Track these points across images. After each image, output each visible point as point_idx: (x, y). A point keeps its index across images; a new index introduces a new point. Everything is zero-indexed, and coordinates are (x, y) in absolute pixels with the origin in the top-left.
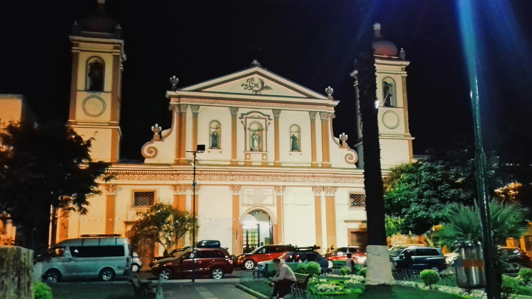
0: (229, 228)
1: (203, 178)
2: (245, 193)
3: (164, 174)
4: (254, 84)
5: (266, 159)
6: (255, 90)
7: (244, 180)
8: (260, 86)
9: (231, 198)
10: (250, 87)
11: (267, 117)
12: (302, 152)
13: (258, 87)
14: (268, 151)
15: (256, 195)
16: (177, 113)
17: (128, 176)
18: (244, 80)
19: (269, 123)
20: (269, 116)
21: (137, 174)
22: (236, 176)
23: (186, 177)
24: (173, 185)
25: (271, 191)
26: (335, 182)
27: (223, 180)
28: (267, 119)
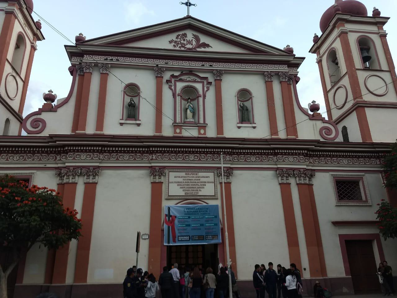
0: (143, 235)
2: (172, 179)
3: (47, 152)
4: (187, 41)
5: (205, 134)
6: (188, 47)
7: (170, 159)
8: (194, 43)
9: (150, 186)
12: (255, 124)
13: (192, 45)
14: (206, 123)
16: (79, 75)
18: (173, 36)
20: (206, 78)
21: (5, 153)
23: (78, 156)
24: (56, 168)
25: (211, 175)
26: (310, 163)
28: (205, 83)
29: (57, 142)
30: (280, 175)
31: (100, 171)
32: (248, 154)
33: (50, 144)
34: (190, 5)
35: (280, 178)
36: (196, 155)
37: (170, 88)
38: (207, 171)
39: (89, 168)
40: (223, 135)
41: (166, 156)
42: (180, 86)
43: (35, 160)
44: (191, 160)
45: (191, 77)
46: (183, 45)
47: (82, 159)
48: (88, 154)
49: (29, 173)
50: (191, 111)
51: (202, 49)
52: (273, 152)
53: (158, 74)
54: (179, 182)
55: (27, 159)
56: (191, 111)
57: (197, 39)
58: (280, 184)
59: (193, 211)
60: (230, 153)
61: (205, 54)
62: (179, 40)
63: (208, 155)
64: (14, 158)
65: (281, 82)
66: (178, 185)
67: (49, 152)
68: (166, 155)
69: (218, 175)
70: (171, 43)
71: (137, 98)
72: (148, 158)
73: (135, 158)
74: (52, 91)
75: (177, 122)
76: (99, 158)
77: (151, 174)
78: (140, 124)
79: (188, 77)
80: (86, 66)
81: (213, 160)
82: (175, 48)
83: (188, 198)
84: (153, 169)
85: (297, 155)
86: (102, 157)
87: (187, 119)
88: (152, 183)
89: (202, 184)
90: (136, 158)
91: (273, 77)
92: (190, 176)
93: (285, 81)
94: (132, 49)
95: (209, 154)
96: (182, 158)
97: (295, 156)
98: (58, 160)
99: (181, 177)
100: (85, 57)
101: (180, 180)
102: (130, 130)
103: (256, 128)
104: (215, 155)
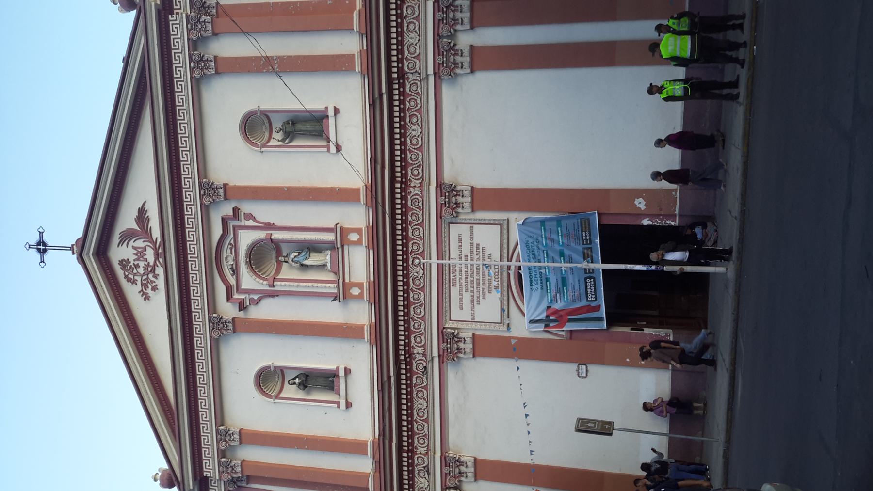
0: (578, 375)
1: (422, 441)
2: (465, 315)
4: (138, 259)
5: (358, 231)
6: (154, 259)
7: (423, 318)
8: (140, 243)
9: (480, 360)
11: (232, 223)
12: (327, 108)
13: (145, 249)
14: (332, 226)
15: (471, 280)
16: (247, 484)
18: (132, 292)
19: (249, 216)
20: (225, 221)
22: (413, 341)
25: (455, 230)
27: (425, 384)
28: (236, 223)
30: (452, 70)
31: (451, 455)
32: (403, 143)
35: (458, 71)
36: (410, 263)
37: (257, 303)
38: (447, 239)
39: (446, 474)
40: (358, 190)
41: (416, 325)
42: (248, 280)
44: (422, 272)
45: (225, 256)
46: (150, 269)
47: (429, 485)
48: (416, 475)
50: (307, 256)
52: (399, 83)
53: (227, 329)
54: (472, 301)
56: (307, 256)
57: (128, 236)
58: (472, 71)
59: (535, 272)
60: (403, 186)
61: (165, 225)
62: (138, 278)
63: (410, 234)
65: (215, 34)
66: (479, 303)
68: (414, 325)
69: (455, 216)
70: (150, 297)
71: (286, 372)
72: (421, 361)
73: (421, 387)
75: (335, 291)
76: (425, 455)
77: (455, 359)
78: (346, 369)
79: (225, 263)
80: (228, 473)
81: (422, 224)
82: (158, 287)
83: (505, 284)
84: (445, 354)
85: (402, 22)
86: (423, 449)
87: (325, 265)
88: (474, 356)
89: (475, 253)
90: (423, 385)
91: (203, 56)
92: (458, 277)
93: (210, 25)
94: (178, 385)
95: (407, 232)
96: (420, 292)
97: (405, 28)
99: (461, 297)
100: (209, 473)
101: (467, 297)
103: (337, 107)
104: (410, 219)
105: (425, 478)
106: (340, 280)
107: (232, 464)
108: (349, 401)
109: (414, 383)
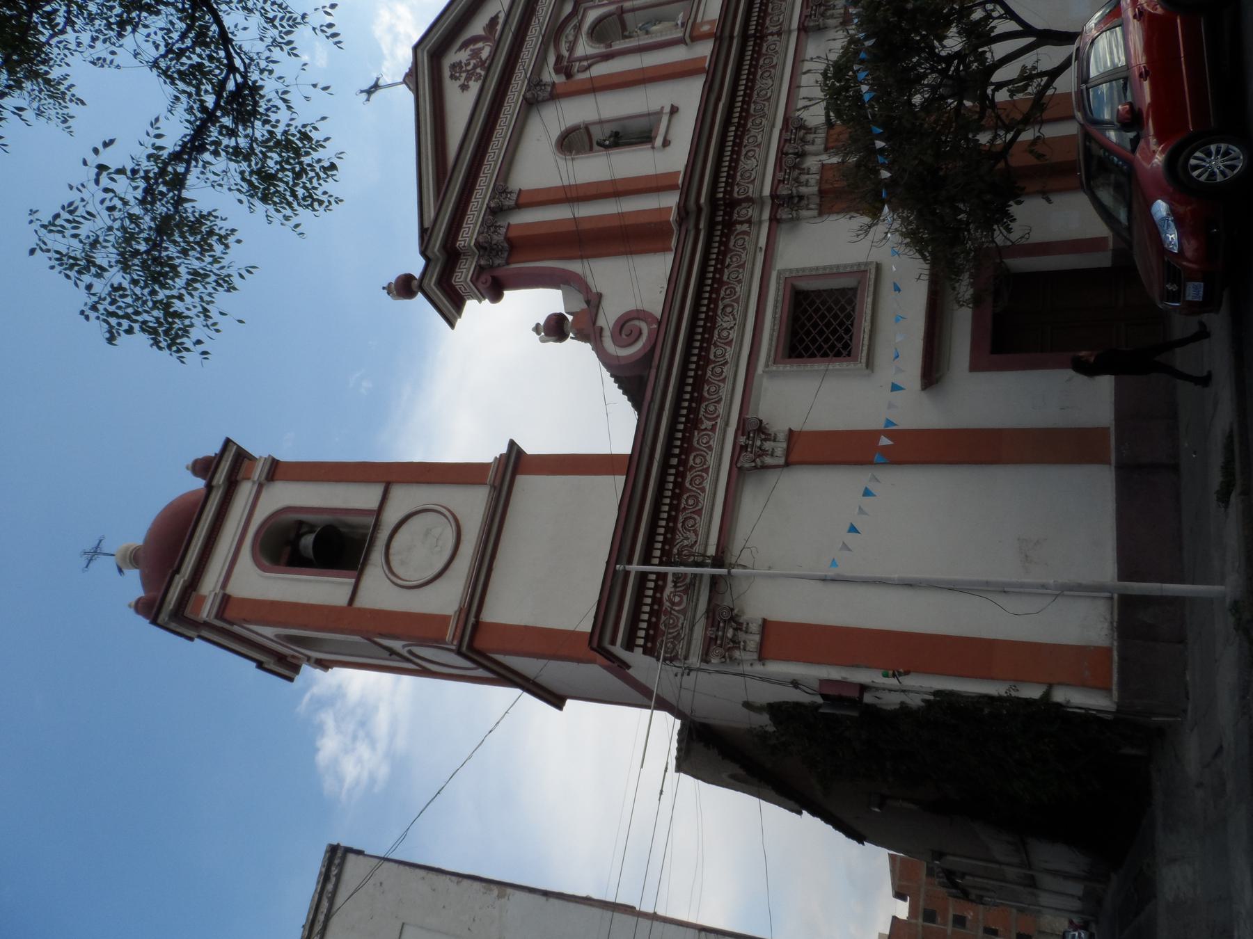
1: (758, 121)
3: (723, 254)
8: (480, 45)
10: (475, 67)
13: (483, 48)
16: (508, 263)
17: (709, 383)
21: (708, 350)
27: (774, 63)
29: (702, 200)
33: (702, 226)
34: (376, 86)
42: (584, 48)
43: (741, 277)
45: (568, 32)
48: (742, 158)
49: (778, 283)
51: (499, 27)
55: (735, 297)
62: (464, 75)
64: (726, 328)
67: (722, 248)
74: (534, 325)
75: (681, 35)
98: (750, 227)
100: (463, 243)
102: (683, 131)
105: (755, 158)
106: (690, 21)
107: (498, 224)
108: (668, 138)
109: (760, 64)
